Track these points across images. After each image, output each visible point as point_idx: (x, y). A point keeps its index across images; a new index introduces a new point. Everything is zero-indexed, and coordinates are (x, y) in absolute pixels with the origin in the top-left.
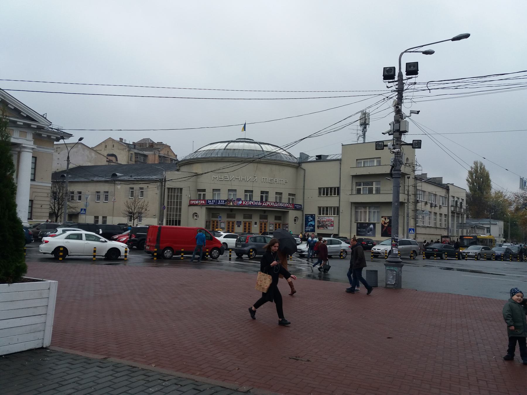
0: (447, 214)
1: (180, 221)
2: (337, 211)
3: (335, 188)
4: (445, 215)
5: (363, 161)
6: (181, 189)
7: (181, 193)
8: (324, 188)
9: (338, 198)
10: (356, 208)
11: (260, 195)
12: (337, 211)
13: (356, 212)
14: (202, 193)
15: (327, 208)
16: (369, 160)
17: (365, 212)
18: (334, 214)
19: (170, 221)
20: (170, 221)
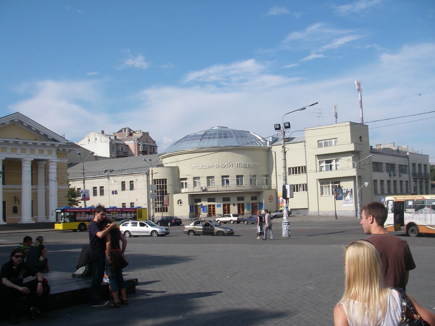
0: (408, 180)
1: (167, 208)
2: (305, 187)
3: (302, 167)
4: (407, 182)
5: (323, 142)
6: (166, 180)
7: (166, 183)
8: (293, 168)
9: (306, 175)
10: (321, 184)
11: (235, 178)
12: (305, 187)
13: (322, 188)
14: (184, 181)
15: (297, 185)
16: (328, 141)
17: (329, 186)
18: (304, 190)
19: (159, 208)
20: (159, 208)
